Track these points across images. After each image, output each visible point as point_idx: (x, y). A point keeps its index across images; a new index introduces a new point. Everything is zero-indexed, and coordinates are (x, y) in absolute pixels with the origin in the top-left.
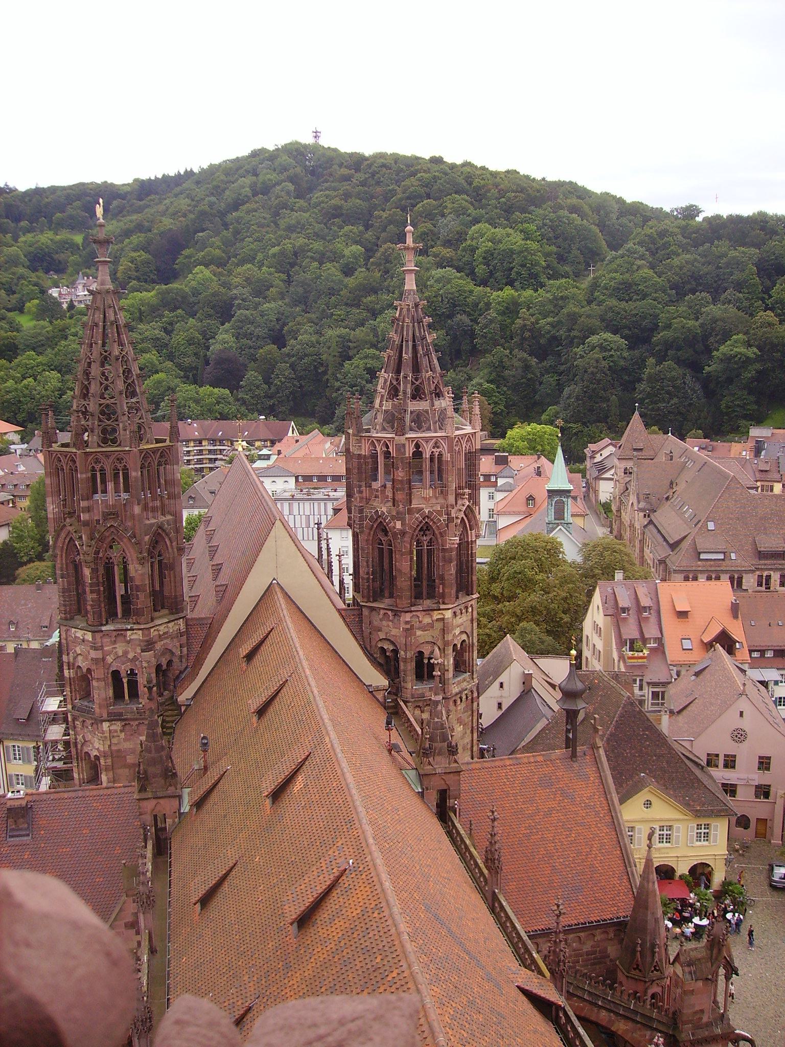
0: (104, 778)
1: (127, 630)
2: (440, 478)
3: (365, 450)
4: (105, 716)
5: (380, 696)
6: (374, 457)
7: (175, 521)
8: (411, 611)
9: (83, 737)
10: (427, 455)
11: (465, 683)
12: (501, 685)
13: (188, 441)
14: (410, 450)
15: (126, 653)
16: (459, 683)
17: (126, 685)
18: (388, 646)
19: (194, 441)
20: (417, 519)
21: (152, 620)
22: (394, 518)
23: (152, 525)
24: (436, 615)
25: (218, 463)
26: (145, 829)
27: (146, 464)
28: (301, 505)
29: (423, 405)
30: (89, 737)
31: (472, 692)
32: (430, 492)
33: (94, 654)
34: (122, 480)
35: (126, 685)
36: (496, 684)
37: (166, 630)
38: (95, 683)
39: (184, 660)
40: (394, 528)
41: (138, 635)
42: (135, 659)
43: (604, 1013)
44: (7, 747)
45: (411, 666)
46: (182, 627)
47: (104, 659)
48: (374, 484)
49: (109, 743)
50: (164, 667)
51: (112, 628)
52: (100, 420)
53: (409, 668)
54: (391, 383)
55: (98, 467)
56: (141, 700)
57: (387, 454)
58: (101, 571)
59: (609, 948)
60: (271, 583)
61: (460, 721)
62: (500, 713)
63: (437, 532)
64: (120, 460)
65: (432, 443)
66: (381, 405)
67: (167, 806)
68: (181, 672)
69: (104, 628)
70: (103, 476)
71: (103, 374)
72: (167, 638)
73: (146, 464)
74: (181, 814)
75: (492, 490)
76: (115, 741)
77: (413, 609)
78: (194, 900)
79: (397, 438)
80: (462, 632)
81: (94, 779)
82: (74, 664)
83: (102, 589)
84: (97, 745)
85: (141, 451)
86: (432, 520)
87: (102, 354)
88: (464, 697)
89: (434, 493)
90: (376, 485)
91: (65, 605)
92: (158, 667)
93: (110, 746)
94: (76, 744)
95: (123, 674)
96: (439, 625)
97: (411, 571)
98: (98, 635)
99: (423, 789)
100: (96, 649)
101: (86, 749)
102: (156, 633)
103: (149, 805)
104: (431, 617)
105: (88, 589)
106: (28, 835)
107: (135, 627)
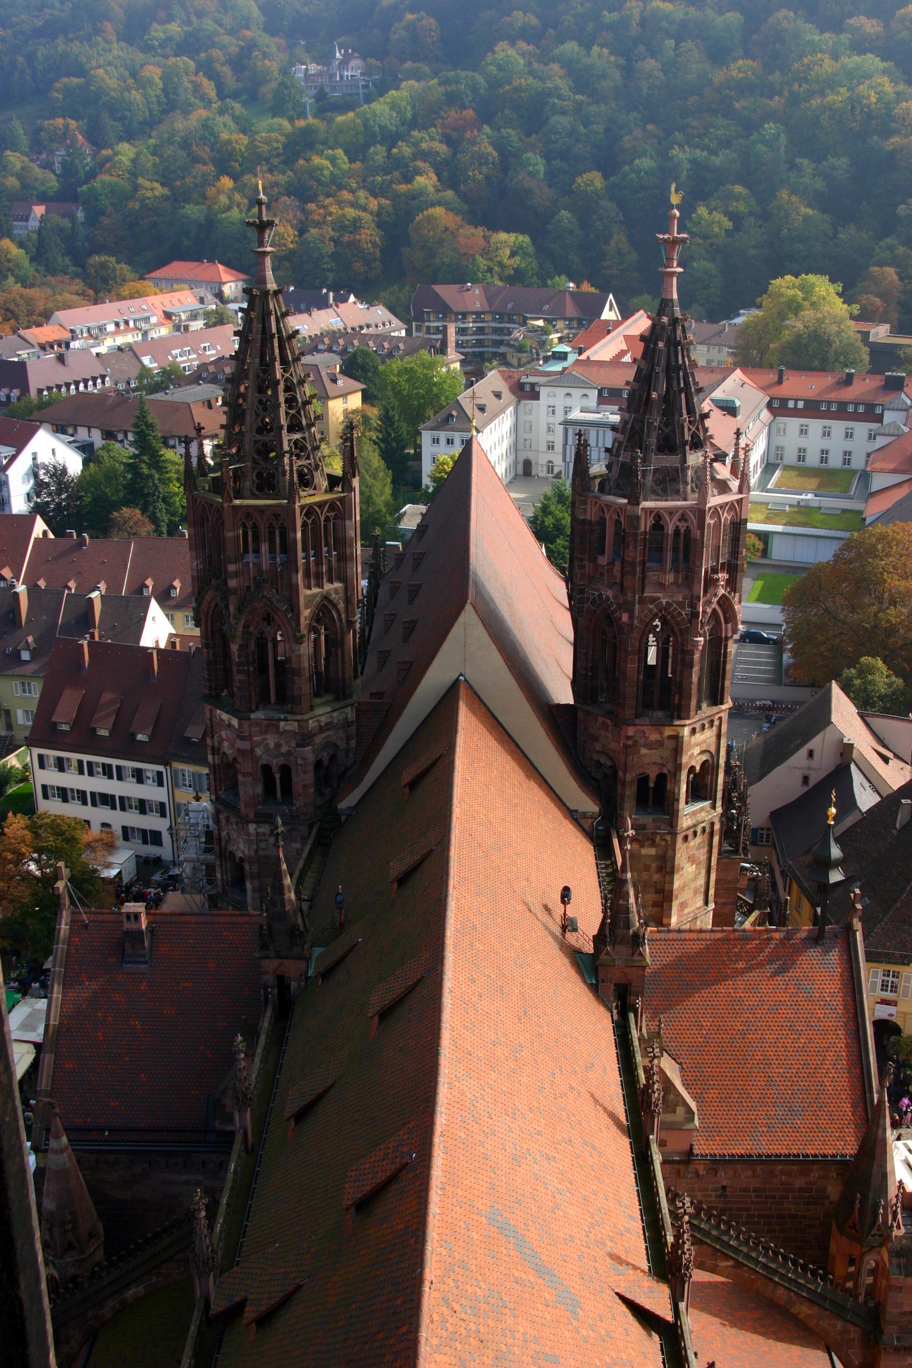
0: (248, 886)
1: (280, 720)
2: (687, 559)
3: (591, 514)
4: (252, 816)
5: (587, 824)
6: (602, 522)
7: (346, 589)
8: (635, 725)
9: (228, 834)
10: (671, 530)
11: (703, 814)
12: (811, 754)
13: (465, 315)
14: (646, 524)
15: (278, 746)
16: (694, 813)
17: (278, 781)
18: (603, 760)
19: (474, 313)
20: (650, 610)
21: (312, 708)
22: (620, 607)
23: (314, 596)
24: (668, 732)
25: (503, 349)
26: (266, 990)
27: (309, 522)
28: (601, 433)
29: (670, 461)
30: (234, 835)
31: (712, 824)
32: (670, 578)
33: (240, 744)
34: (278, 541)
35: (278, 781)
36: (803, 752)
37: (329, 720)
38: (240, 778)
39: (351, 755)
40: (620, 619)
41: (292, 726)
42: (289, 753)
43: (781, 1291)
44: (176, 771)
45: (630, 792)
46: (349, 716)
47: (252, 751)
48: (600, 558)
49: (255, 847)
50: (326, 763)
51: (263, 717)
52: (255, 462)
53: (628, 793)
54: (633, 427)
55: (249, 524)
56: (294, 802)
57: (618, 522)
58: (253, 647)
59: (829, 1188)
60: (457, 680)
61: (692, 859)
62: (805, 789)
63: (676, 629)
64: (276, 516)
65: (676, 517)
66: (618, 455)
67: (291, 968)
68: (347, 769)
69: (253, 716)
70: (256, 539)
71: (260, 402)
72: (328, 730)
73: (309, 522)
74: (307, 978)
75: (874, 426)
76: (263, 845)
77: (637, 721)
78: (287, 1114)
79: (629, 507)
80: (702, 752)
81: (239, 883)
82: (219, 750)
83: (252, 669)
84: (242, 846)
85: (302, 507)
86: (670, 613)
87: (258, 376)
88: (699, 829)
89: (676, 578)
90: (603, 560)
91: (210, 680)
92: (318, 764)
93: (256, 851)
94: (219, 840)
95: (275, 769)
96: (670, 744)
97: (639, 674)
98: (246, 724)
99: (597, 980)
100: (242, 738)
101: (231, 848)
102: (316, 724)
103: (271, 965)
104: (661, 733)
105: (234, 668)
106: (146, 963)
107: (290, 717)
